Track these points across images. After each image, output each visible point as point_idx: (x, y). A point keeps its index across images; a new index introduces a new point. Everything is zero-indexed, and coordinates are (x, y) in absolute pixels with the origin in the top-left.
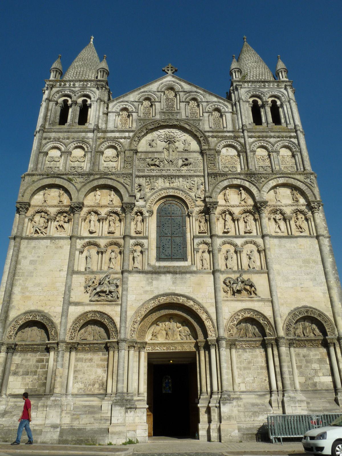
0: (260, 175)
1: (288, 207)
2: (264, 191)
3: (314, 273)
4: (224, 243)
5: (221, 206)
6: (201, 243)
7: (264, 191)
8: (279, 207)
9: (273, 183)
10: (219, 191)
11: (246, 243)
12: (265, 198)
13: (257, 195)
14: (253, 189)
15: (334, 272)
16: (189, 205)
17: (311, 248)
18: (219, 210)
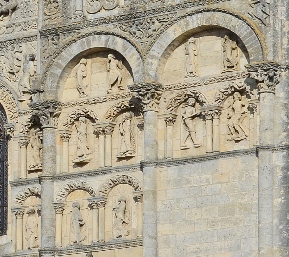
0: (150, 16)
1: (212, 86)
2: (153, 57)
3: (239, 234)
4: (71, 190)
5: (68, 105)
6: (27, 196)
7: (153, 57)
8: (190, 89)
9: (175, 30)
10: (59, 71)
11: (114, 184)
12: (153, 74)
13: (136, 69)
14: (131, 54)
15: (281, 227)
16: (7, 113)
17: (244, 179)
18: (66, 114)
